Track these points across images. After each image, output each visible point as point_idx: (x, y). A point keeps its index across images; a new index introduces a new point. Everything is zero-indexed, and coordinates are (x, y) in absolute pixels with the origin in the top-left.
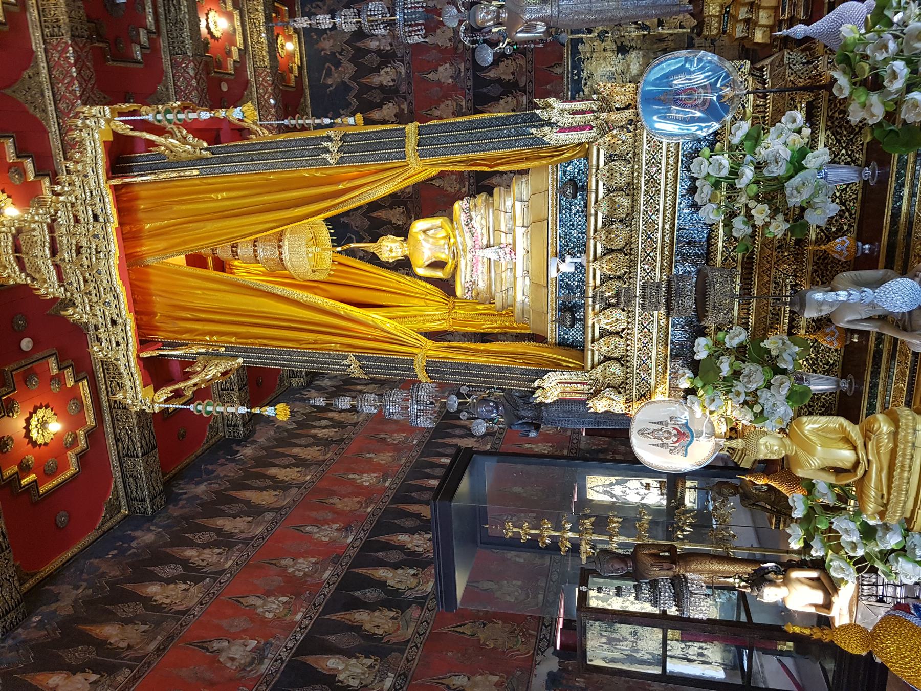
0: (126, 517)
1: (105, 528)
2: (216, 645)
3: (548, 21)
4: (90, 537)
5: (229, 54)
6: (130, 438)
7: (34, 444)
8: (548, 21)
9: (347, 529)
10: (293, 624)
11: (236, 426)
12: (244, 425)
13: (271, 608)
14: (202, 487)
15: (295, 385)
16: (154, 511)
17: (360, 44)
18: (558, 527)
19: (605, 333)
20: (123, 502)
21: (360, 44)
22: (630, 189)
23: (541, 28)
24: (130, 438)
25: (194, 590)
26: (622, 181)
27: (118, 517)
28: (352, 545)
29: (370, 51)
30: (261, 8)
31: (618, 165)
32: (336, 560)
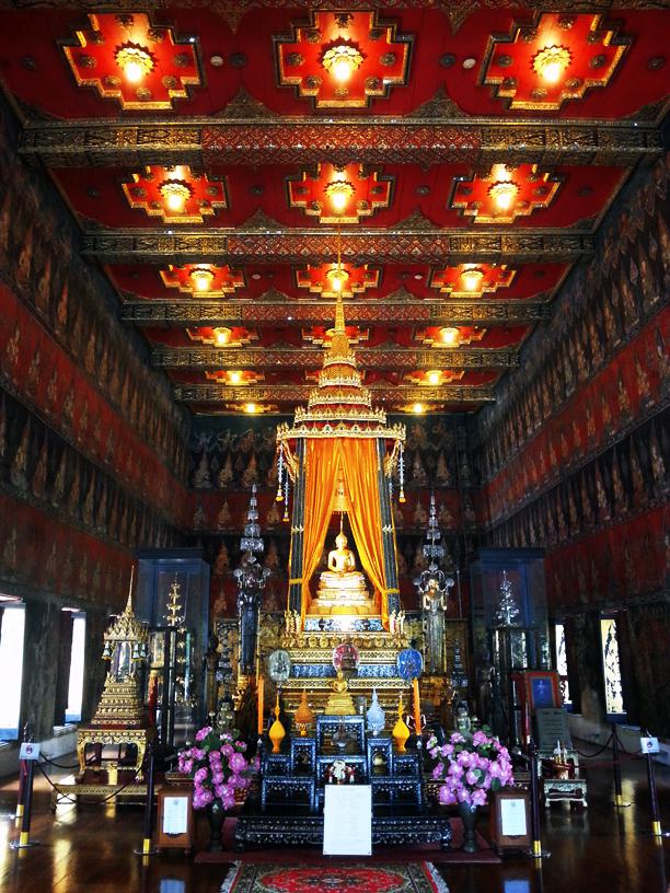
0: (120, 302)
1: (120, 293)
2: (72, 392)
3: (430, 611)
4: (117, 286)
5: (416, 377)
6: (179, 314)
7: (194, 270)
8: (430, 611)
9: (110, 459)
10: (76, 436)
11: (161, 361)
12: (162, 367)
13: (83, 422)
14: (131, 347)
15: (176, 391)
16: (124, 321)
17: (417, 456)
18: (179, 613)
19: (318, 640)
20: (133, 303)
21: (417, 456)
22: (374, 647)
23: (428, 608)
24: (179, 314)
25: (92, 368)
26: (377, 644)
27: (123, 298)
28: (105, 464)
29: (413, 462)
30: (443, 398)
31: (382, 642)
32: (98, 455)
